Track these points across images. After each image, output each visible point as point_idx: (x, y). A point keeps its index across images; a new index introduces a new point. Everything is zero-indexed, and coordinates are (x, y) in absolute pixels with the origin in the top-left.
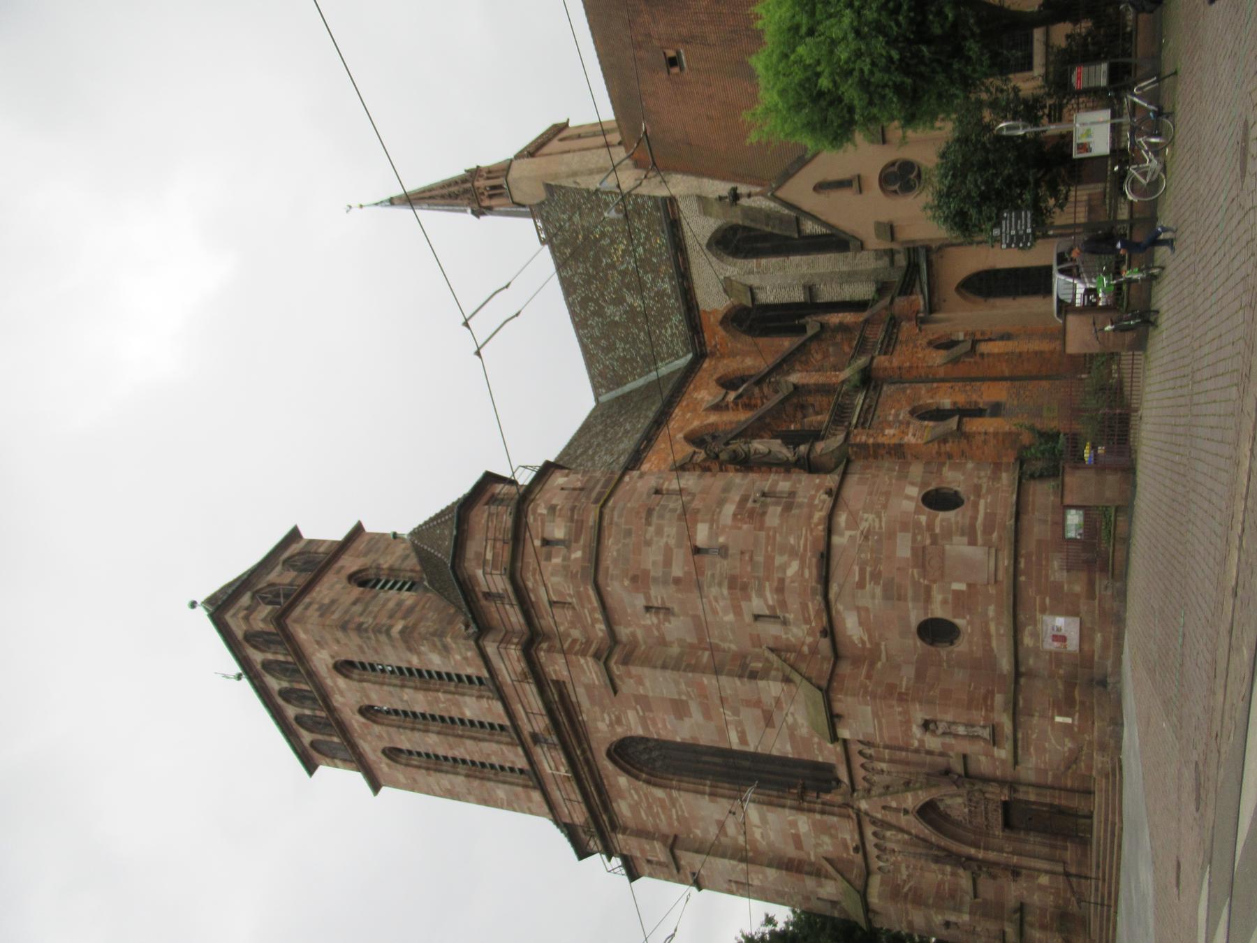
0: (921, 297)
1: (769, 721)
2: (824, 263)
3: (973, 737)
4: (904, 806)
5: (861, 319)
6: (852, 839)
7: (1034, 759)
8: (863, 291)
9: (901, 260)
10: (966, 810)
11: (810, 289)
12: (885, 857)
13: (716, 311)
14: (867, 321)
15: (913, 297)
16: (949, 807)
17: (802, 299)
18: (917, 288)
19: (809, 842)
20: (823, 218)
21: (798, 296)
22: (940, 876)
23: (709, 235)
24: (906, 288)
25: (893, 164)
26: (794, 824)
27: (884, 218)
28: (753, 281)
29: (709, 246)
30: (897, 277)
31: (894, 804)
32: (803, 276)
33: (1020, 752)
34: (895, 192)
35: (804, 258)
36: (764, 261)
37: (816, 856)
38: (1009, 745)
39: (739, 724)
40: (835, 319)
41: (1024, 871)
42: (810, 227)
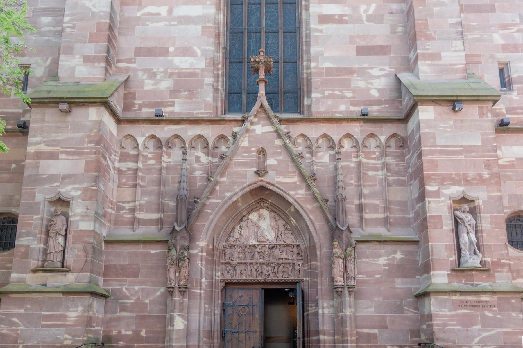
1: (362, 51)
3: (459, 250)
4: (271, 173)
6: (173, 113)
7: (447, 312)
10: (255, 243)
12: (151, 144)
16: (255, 225)
19: (156, 64)
22: (127, 206)
26: (186, 51)
31: (271, 162)
33: (457, 298)
37: (127, 70)
38: (456, 285)
39: (359, 20)
41: (186, 300)
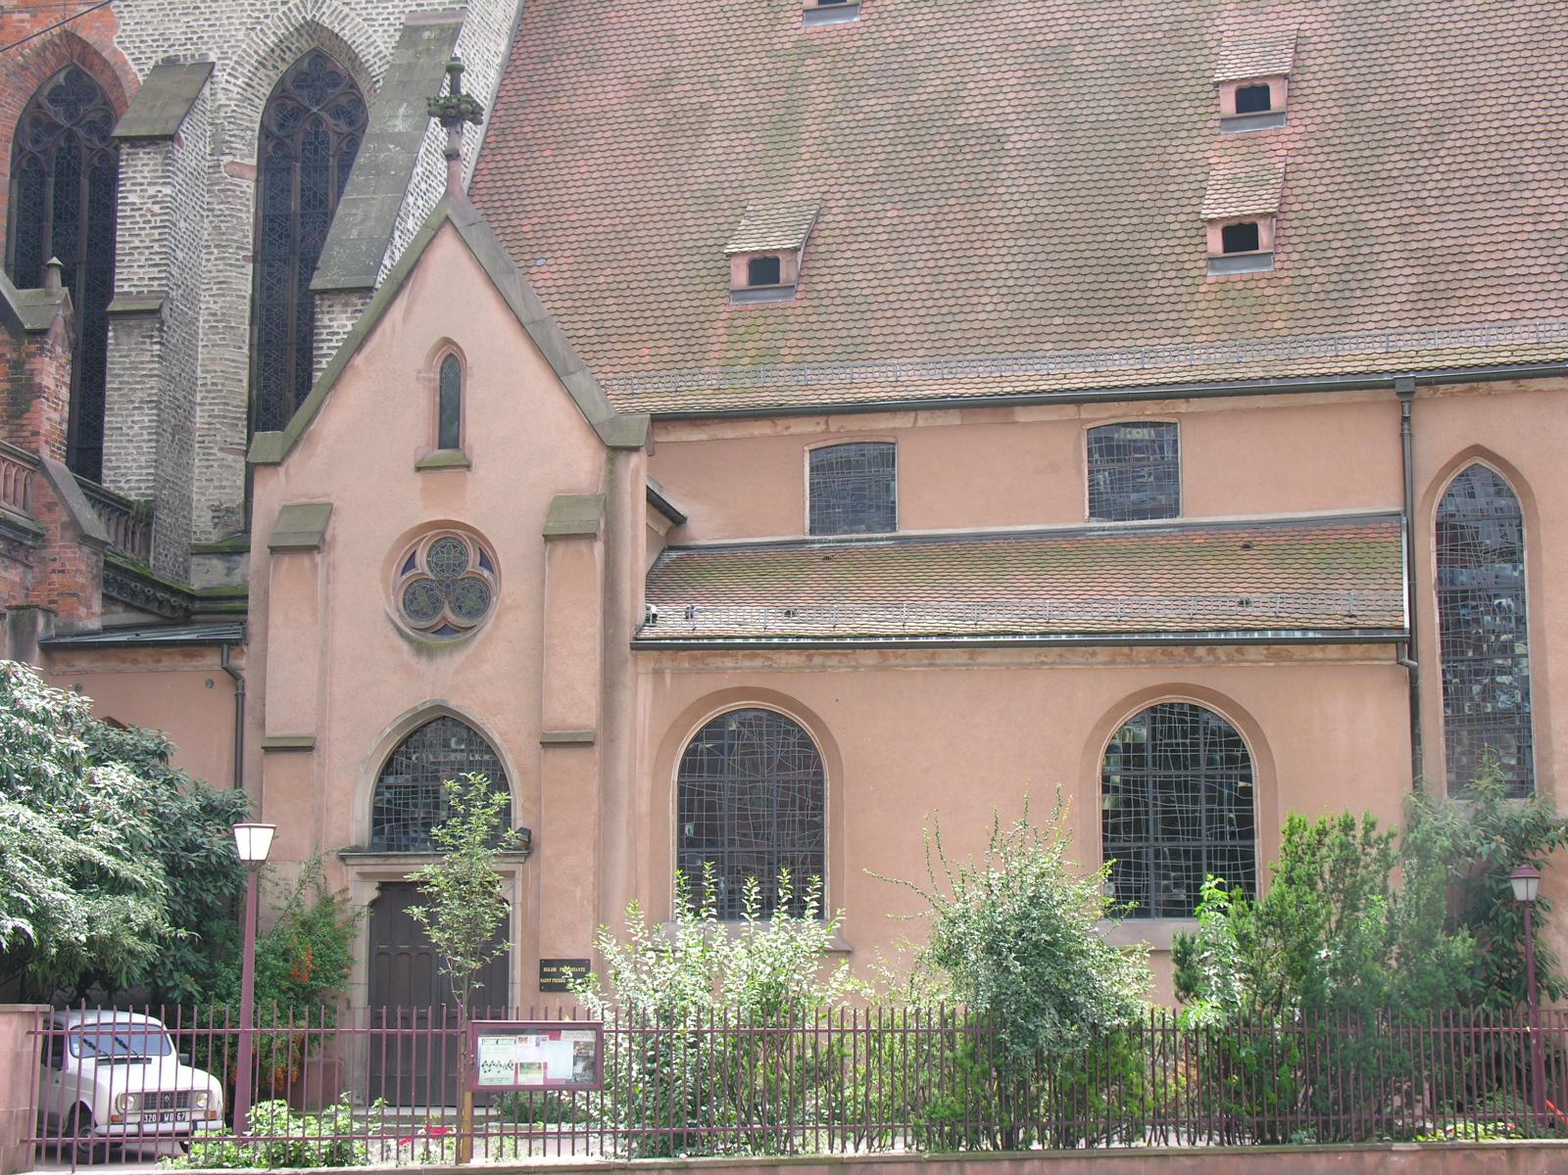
0: (95, 624)
2: (224, 360)
5: (45, 453)
8: (128, 466)
9: (206, 576)
11: (149, 315)
13: (112, 27)
14: (38, 464)
15: (97, 606)
17: (122, 286)
18: (122, 617)
20: (359, 360)
21: (134, 275)
23: (346, 35)
24: (123, 584)
25: (485, 562)
27: (341, 529)
28: (193, 149)
29: (312, 28)
30: (161, 563)
32: (191, 298)
34: (410, 564)
35: (246, 306)
36: (248, 186)
40: (53, 373)
42: (337, 324)
